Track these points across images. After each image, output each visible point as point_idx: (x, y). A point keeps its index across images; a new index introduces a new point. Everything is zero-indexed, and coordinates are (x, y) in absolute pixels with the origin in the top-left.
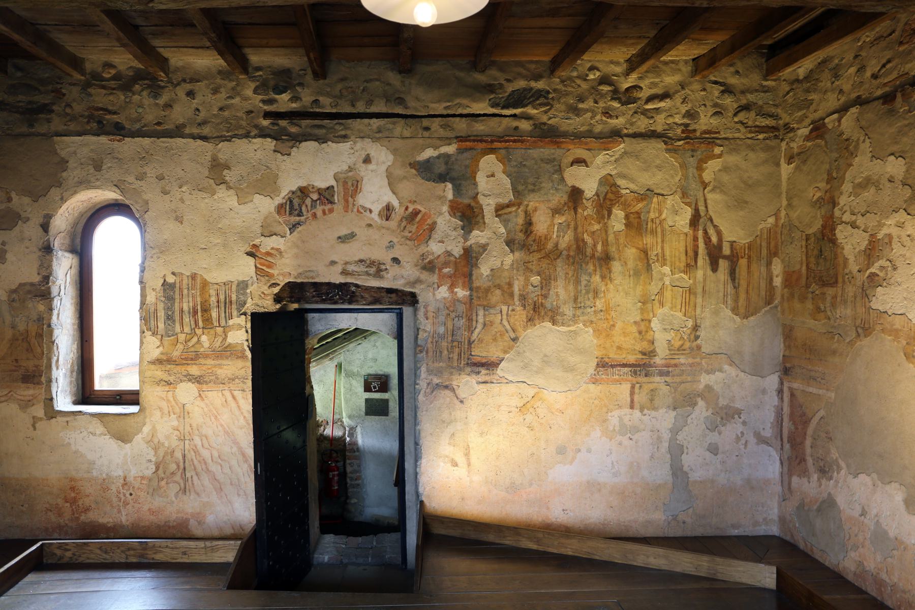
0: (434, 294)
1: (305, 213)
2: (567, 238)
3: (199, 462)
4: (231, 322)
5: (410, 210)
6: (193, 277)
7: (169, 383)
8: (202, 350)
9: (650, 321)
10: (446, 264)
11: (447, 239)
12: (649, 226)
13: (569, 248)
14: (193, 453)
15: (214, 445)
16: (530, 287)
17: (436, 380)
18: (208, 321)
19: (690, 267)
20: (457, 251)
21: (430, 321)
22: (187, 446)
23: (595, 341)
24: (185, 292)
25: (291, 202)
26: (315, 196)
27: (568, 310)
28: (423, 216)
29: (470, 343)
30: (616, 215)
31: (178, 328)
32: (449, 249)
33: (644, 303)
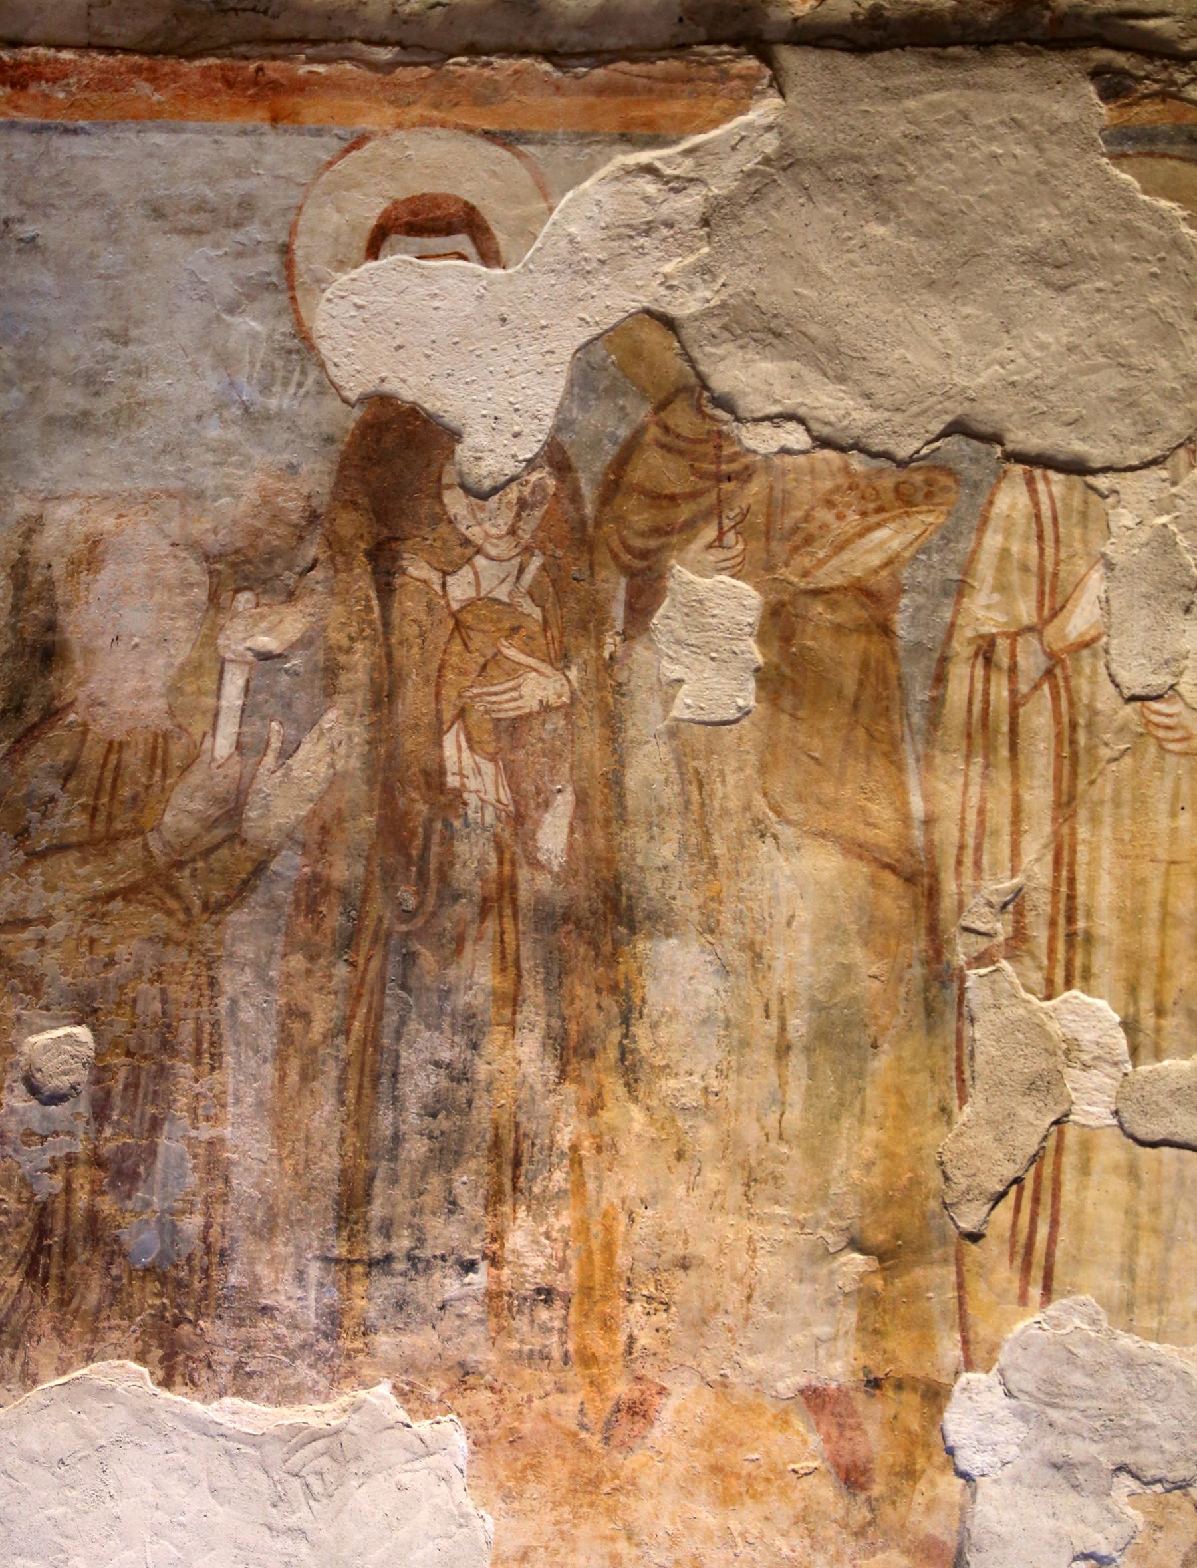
2: (312, 762)
9: (935, 1396)
12: (957, 691)
13: (321, 834)
23: (487, 1525)
27: (287, 1281)
30: (696, 607)
33: (889, 1257)
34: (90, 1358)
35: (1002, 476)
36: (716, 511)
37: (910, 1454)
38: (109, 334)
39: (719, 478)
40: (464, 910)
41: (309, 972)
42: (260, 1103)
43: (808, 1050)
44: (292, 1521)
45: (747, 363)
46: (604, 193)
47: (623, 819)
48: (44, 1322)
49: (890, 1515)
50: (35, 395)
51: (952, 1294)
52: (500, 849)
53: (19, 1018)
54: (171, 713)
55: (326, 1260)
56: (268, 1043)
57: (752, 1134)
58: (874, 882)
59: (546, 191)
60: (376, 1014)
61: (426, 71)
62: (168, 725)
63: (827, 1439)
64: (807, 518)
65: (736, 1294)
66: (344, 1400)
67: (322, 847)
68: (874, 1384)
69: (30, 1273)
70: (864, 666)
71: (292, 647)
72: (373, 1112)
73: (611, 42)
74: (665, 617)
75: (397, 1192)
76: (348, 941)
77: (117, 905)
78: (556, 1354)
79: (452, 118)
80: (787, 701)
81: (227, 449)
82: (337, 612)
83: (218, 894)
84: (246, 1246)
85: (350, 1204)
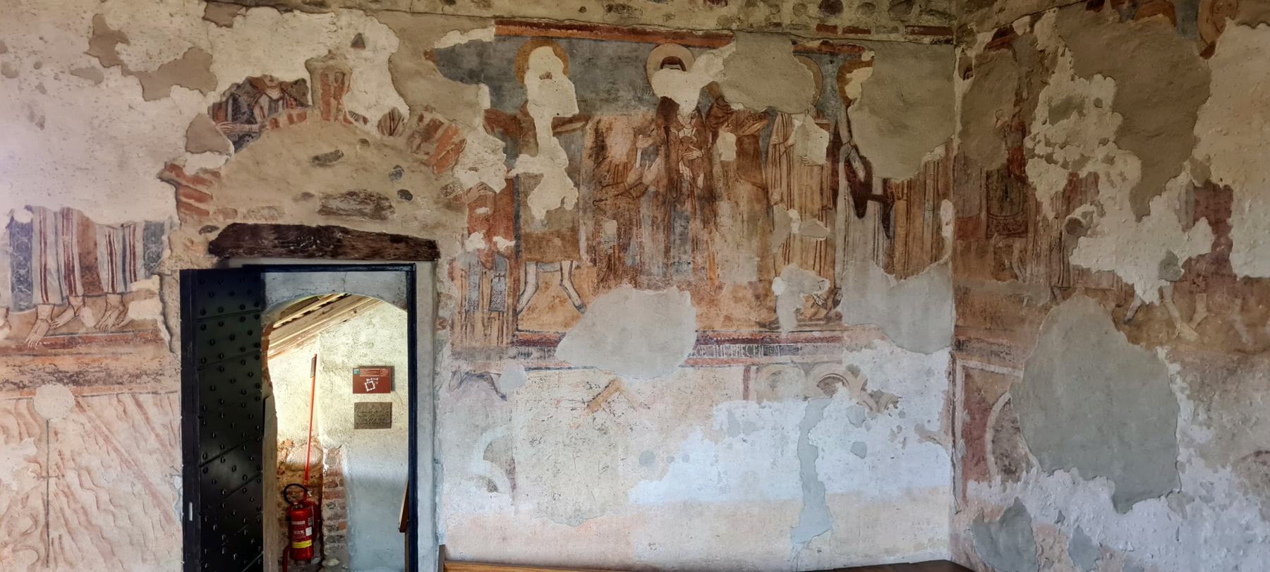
0: (463, 244)
1: (259, 119)
2: (654, 167)
3: (75, 511)
4: (134, 287)
5: (427, 120)
6: (66, 214)
7: (20, 387)
8: (82, 331)
9: (771, 283)
10: (481, 201)
11: (482, 163)
13: (657, 182)
14: (63, 499)
15: (103, 482)
17: (465, 367)
18: (92, 287)
19: (827, 211)
20: (498, 185)
21: (458, 282)
22: (52, 488)
24: (51, 238)
25: (235, 100)
26: (275, 94)
28: (446, 131)
29: (516, 313)
31: (37, 296)
32: (484, 180)
74: (719, 141)
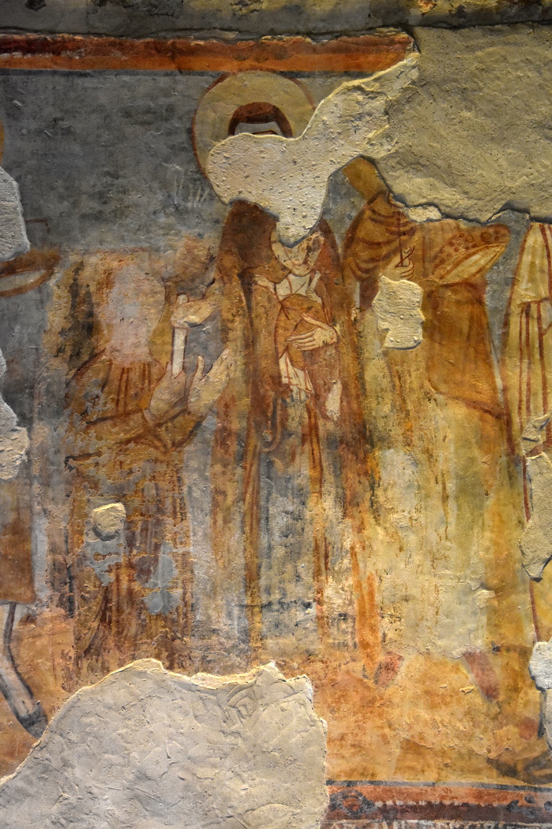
2: (218, 374)
9: (525, 654)
12: (514, 329)
13: (225, 407)
16: (91, 539)
23: (324, 724)
27: (224, 617)
30: (392, 295)
33: (499, 591)
34: (134, 658)
35: (529, 228)
36: (399, 250)
37: (515, 681)
38: (108, 174)
39: (400, 234)
40: (294, 440)
41: (224, 473)
42: (205, 535)
43: (457, 498)
44: (233, 728)
45: (410, 179)
46: (338, 100)
47: (364, 394)
48: (111, 642)
49: (507, 709)
50: (75, 204)
51: (529, 606)
52: (309, 411)
53: (89, 500)
54: (151, 354)
55: (242, 606)
56: (207, 506)
57: (433, 537)
58: (482, 419)
59: (312, 101)
60: (257, 492)
61: (252, 43)
62: (149, 359)
63: (477, 676)
64: (441, 251)
65: (431, 612)
66: (254, 671)
67: (226, 415)
68: (497, 649)
69: (103, 620)
70: (471, 319)
71: (206, 320)
72: (258, 536)
73: (338, 28)
74: (379, 300)
75: (271, 573)
76: (241, 457)
77: (132, 445)
78: (350, 644)
79: (266, 65)
80: (437, 337)
81: (169, 228)
82: (226, 303)
83: (179, 438)
84: (203, 601)
85: (251, 578)
